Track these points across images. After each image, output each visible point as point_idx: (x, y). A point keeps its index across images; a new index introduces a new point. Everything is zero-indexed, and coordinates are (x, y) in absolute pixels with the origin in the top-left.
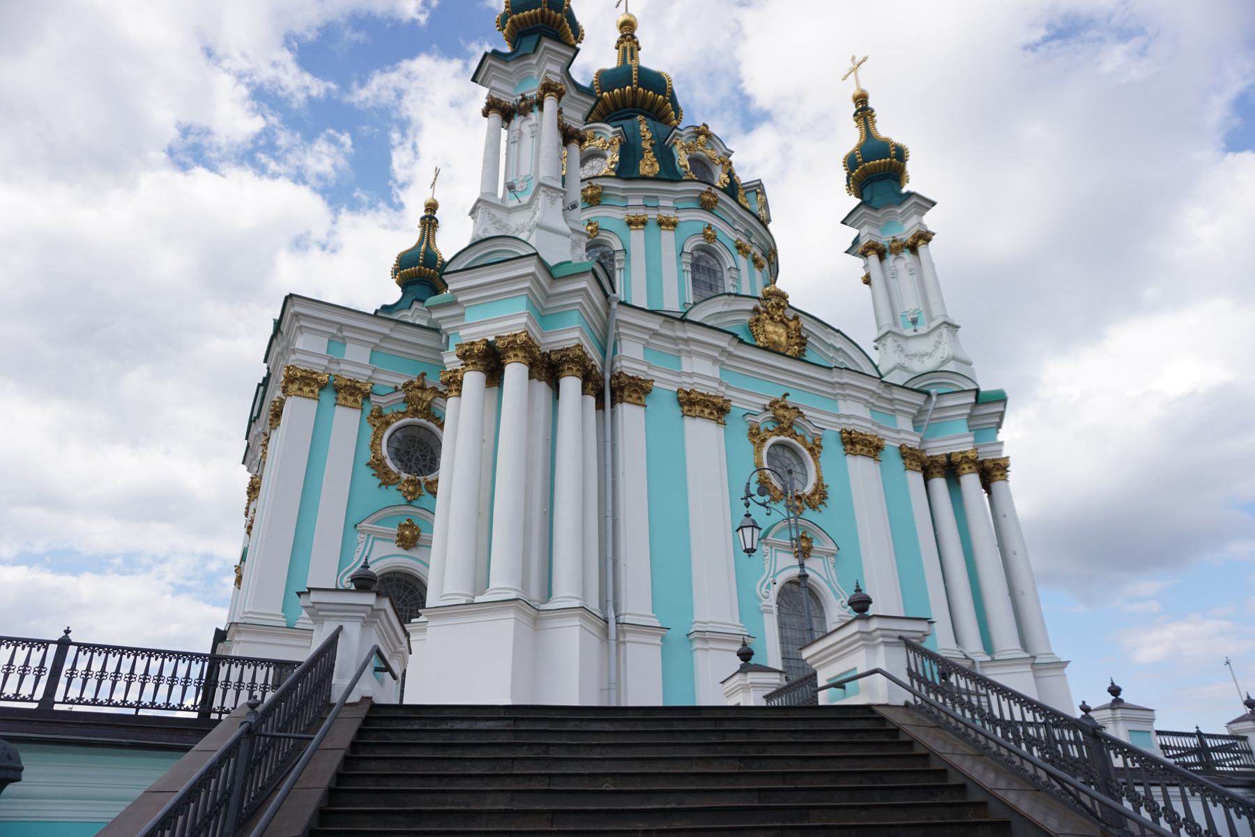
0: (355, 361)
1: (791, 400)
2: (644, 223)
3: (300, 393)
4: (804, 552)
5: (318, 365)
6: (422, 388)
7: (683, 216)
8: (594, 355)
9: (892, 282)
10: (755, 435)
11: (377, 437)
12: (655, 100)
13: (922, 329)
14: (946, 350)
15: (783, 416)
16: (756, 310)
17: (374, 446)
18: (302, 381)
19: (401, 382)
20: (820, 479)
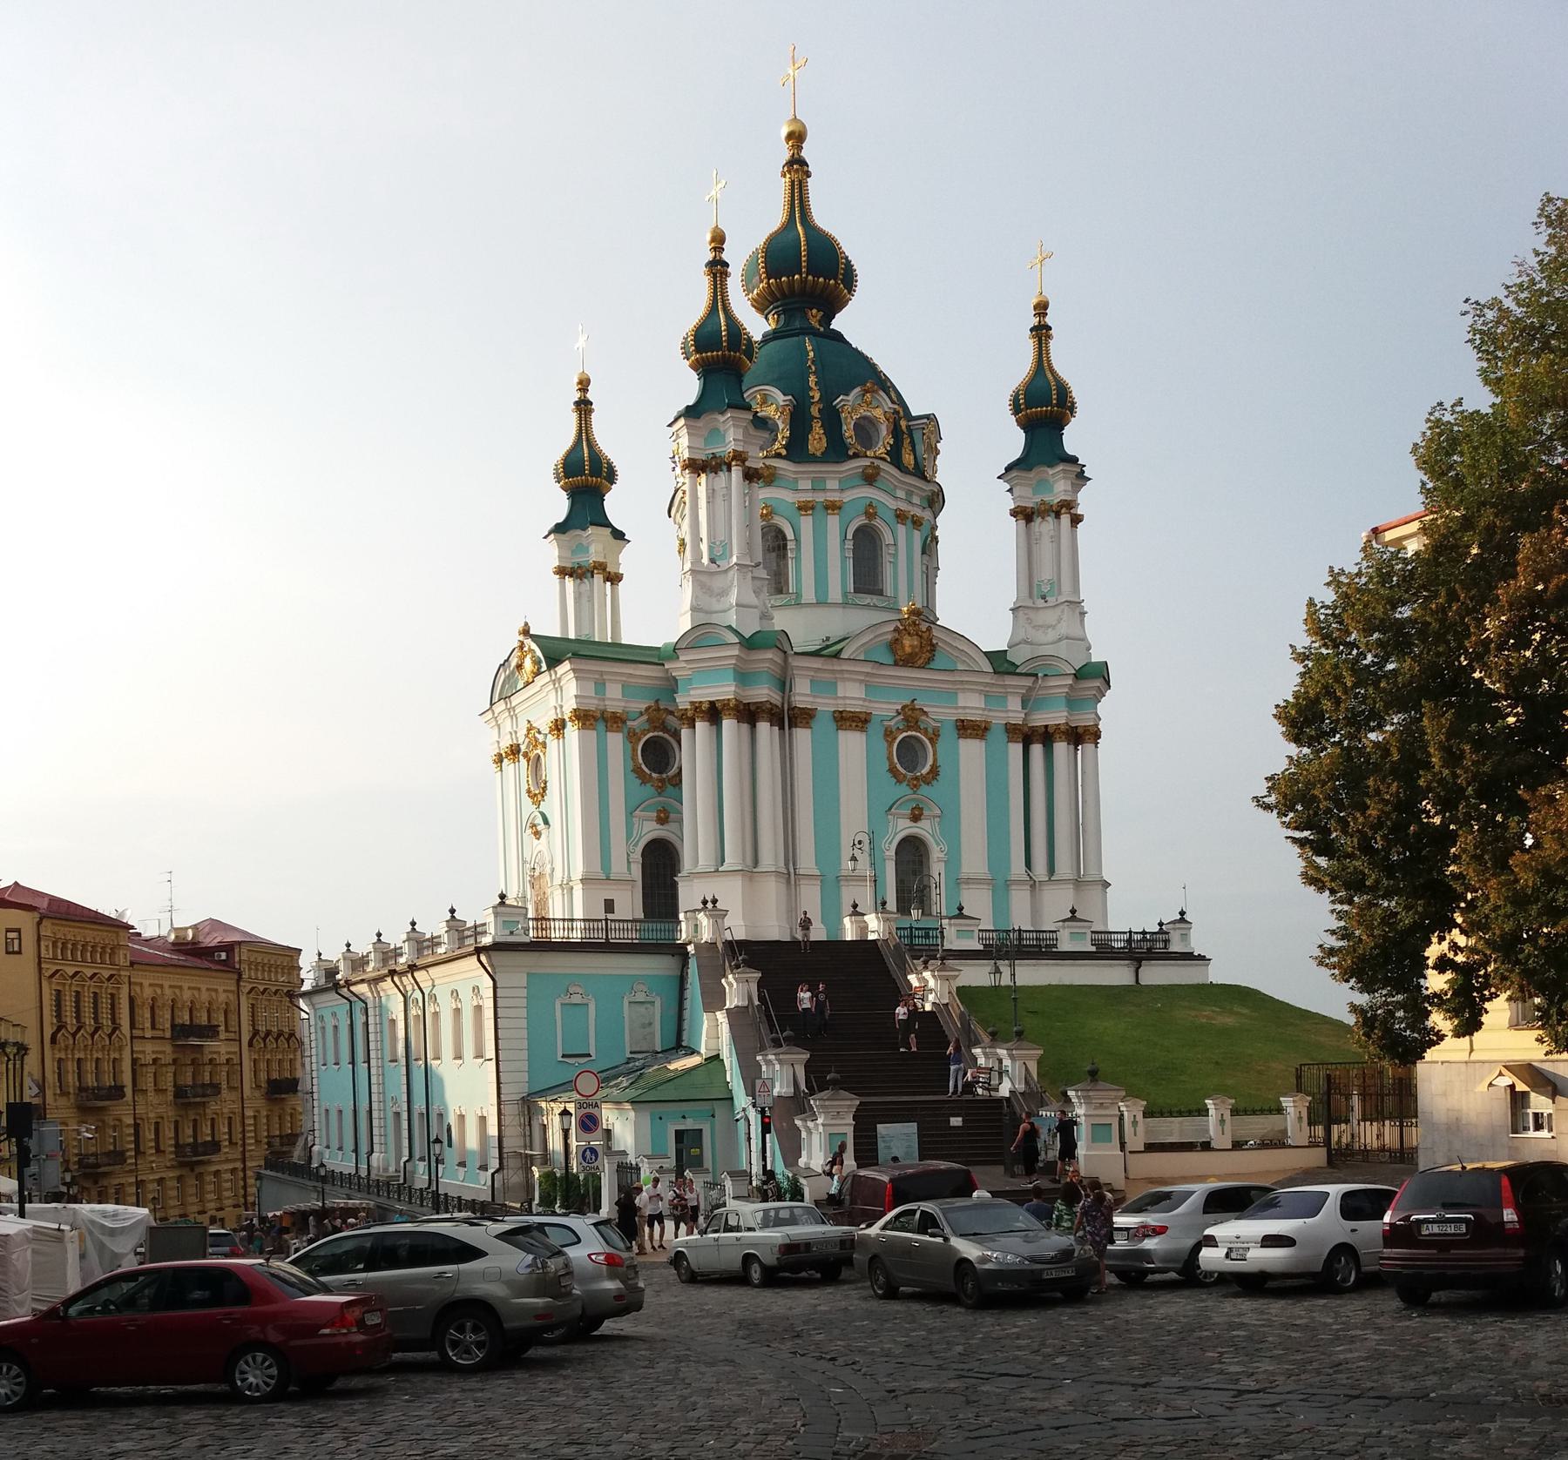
0: (615, 698)
1: (918, 704)
2: (813, 508)
3: (584, 727)
4: (916, 817)
5: (592, 705)
6: (658, 709)
7: (847, 497)
8: (776, 698)
9: (1034, 548)
10: (889, 734)
11: (634, 750)
12: (826, 286)
13: (1051, 600)
14: (1063, 629)
15: (912, 716)
16: (896, 630)
17: (634, 757)
18: (584, 717)
19: (643, 706)
20: (935, 760)
